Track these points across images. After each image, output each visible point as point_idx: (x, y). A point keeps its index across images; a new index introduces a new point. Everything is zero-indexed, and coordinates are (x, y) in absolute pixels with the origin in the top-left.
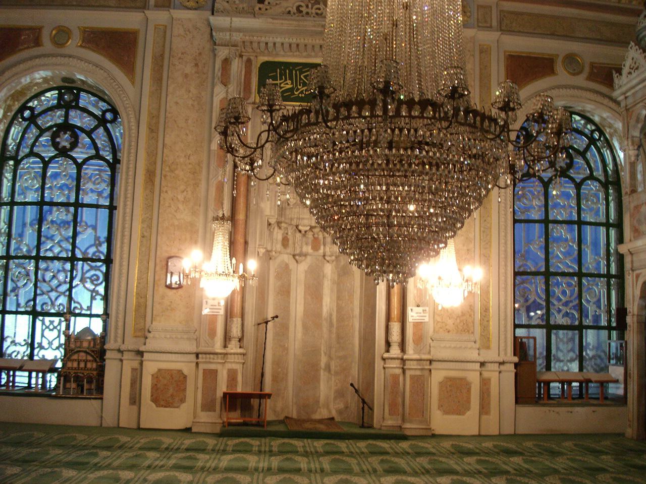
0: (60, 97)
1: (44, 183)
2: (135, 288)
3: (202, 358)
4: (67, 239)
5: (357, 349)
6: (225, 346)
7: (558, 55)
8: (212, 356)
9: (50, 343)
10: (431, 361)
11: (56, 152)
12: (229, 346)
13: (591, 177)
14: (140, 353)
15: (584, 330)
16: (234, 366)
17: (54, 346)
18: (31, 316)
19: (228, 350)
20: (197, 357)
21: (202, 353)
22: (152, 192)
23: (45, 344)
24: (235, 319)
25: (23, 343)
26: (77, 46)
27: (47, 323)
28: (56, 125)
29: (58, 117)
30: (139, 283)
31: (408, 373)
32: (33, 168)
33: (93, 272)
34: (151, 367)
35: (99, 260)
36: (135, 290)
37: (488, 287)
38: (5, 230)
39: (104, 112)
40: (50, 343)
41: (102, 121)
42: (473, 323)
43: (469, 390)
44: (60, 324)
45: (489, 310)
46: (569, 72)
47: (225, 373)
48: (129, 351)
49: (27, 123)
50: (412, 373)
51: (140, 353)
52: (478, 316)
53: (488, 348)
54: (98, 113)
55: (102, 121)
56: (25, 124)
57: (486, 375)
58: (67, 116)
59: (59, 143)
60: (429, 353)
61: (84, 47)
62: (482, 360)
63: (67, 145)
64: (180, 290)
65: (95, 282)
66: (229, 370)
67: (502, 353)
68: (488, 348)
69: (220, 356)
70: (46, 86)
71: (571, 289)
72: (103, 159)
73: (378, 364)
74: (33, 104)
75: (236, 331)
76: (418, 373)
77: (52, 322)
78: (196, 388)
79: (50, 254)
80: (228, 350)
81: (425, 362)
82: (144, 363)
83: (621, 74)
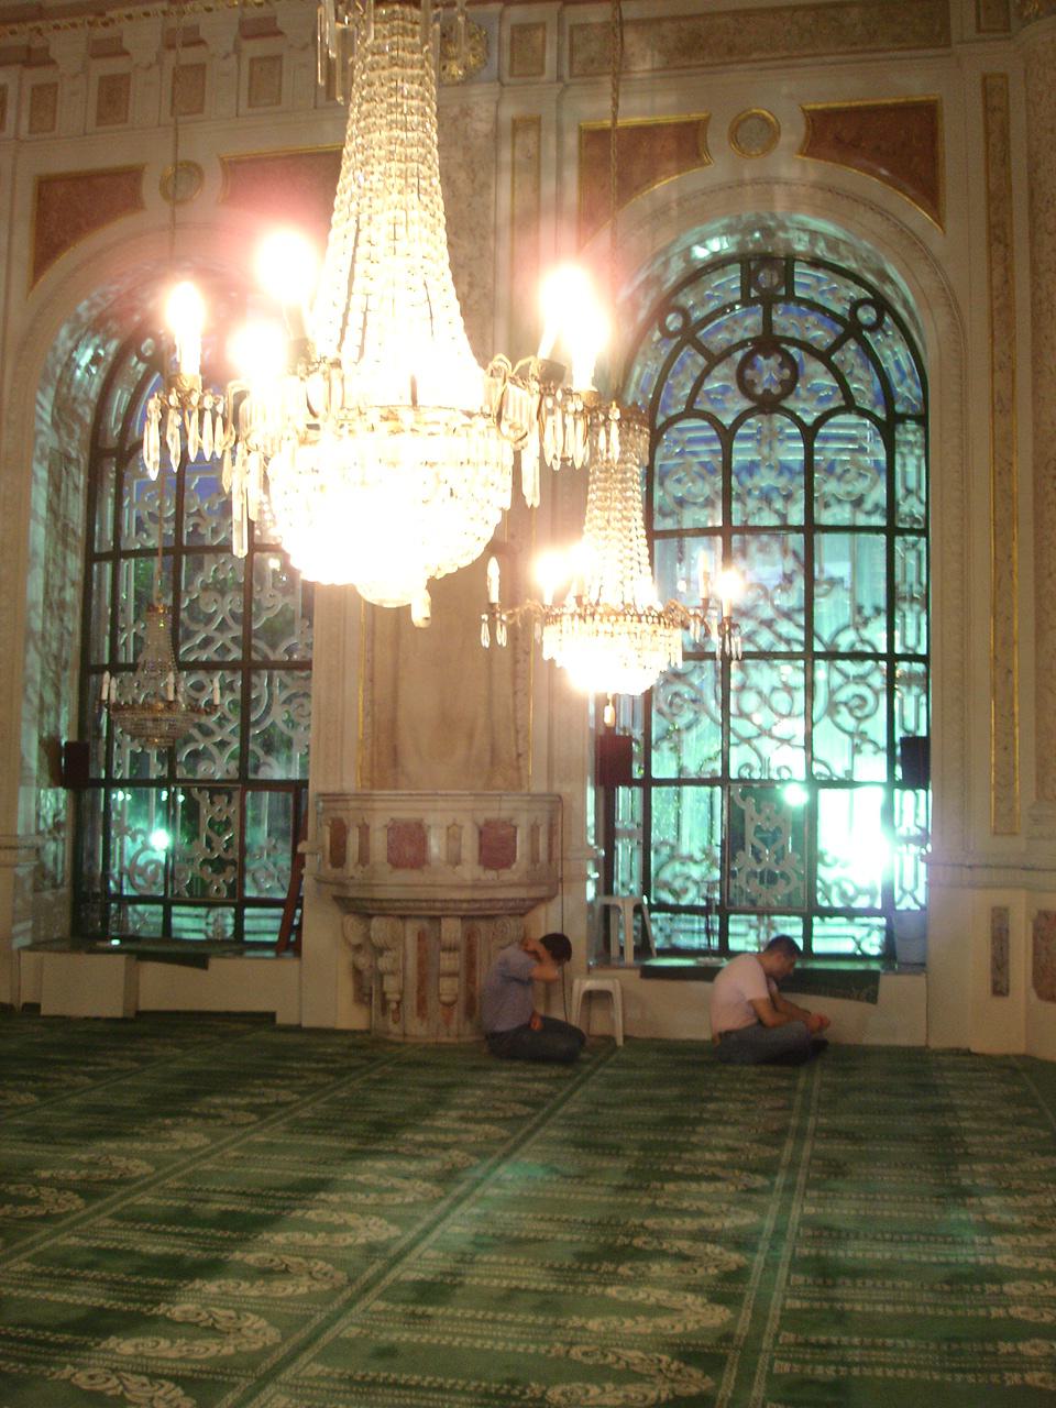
0: (748, 280)
4: (787, 615)
25: (698, 855)
29: (749, 323)
32: (695, 454)
33: (852, 689)
39: (857, 304)
41: (851, 329)
54: (840, 309)
55: (851, 329)
63: (776, 390)
65: (859, 713)
72: (863, 413)
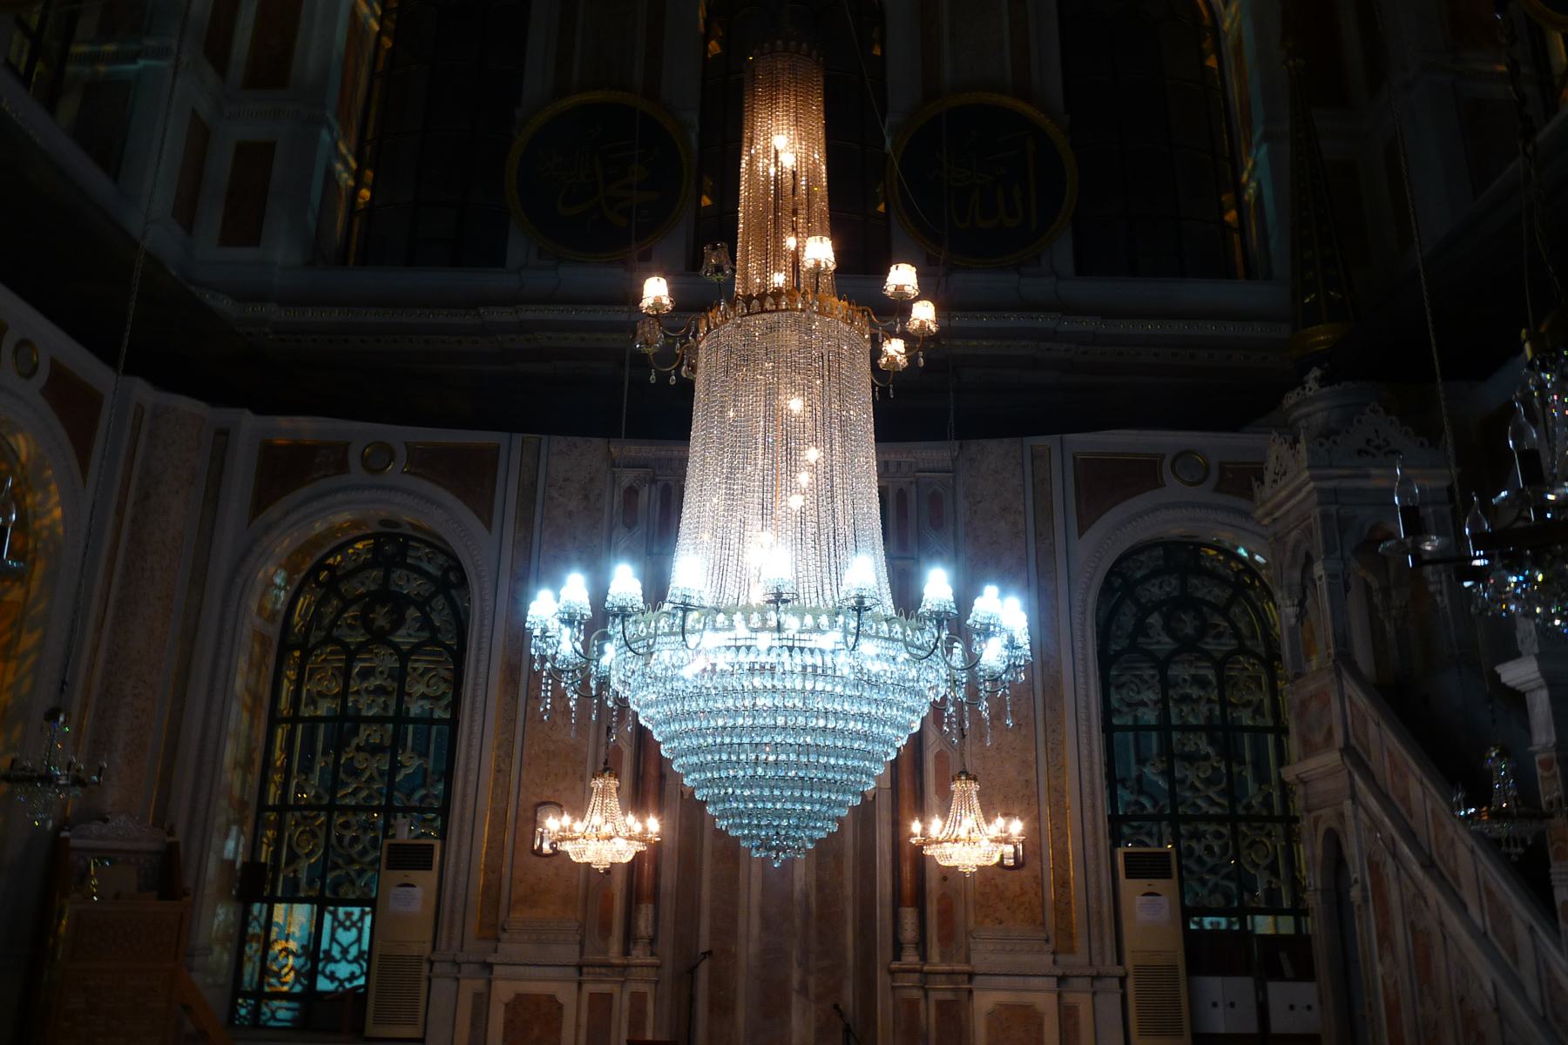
1: (346, 685)
2: (484, 856)
3: (589, 974)
5: (850, 955)
6: (626, 952)
7: (1163, 456)
8: (603, 970)
9: (345, 951)
10: (971, 976)
11: (369, 637)
12: (634, 952)
13: (1242, 650)
14: (488, 967)
15: (1249, 917)
16: (642, 988)
17: (350, 957)
18: (315, 906)
19: (633, 960)
20: (581, 974)
21: (587, 966)
22: (515, 697)
23: (336, 952)
24: (643, 906)
26: (403, 472)
27: (341, 915)
28: (368, 594)
30: (489, 847)
31: (934, 996)
34: (504, 991)
35: (432, 810)
36: (483, 860)
37: (1066, 843)
38: (282, 763)
40: (345, 951)
42: (1043, 905)
43: (1041, 1026)
44: (361, 919)
45: (1069, 883)
46: (1183, 481)
47: (626, 997)
48: (469, 962)
49: (323, 590)
50: (940, 996)
51: (488, 967)
52: (1051, 894)
53: (1071, 951)
56: (320, 592)
57: (1070, 998)
58: (387, 578)
59: (373, 620)
60: (968, 960)
61: (415, 474)
62: (1059, 972)
63: (387, 627)
64: (555, 857)
66: (633, 994)
67: (1096, 960)
68: (1071, 951)
69: (617, 969)
70: (357, 533)
71: (1220, 842)
73: (882, 979)
74: (335, 560)
75: (644, 925)
76: (949, 996)
77: (349, 915)
78: (578, 1026)
79: (351, 801)
80: (633, 960)
81: (960, 978)
82: (493, 983)
83: (1263, 483)
